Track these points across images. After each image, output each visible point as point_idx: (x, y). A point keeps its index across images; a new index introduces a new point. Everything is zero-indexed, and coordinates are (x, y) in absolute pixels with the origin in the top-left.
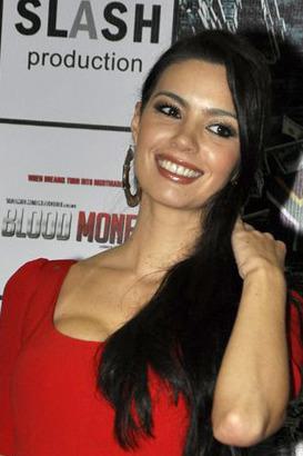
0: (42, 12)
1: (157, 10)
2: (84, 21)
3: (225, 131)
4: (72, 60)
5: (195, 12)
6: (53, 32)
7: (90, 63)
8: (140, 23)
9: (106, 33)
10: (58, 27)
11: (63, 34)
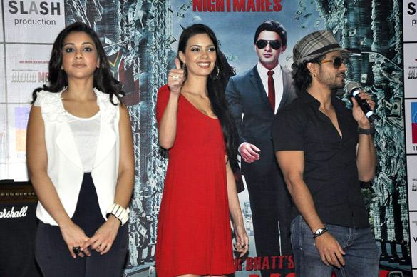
0: (18, 6)
1: (58, 4)
2: (33, 8)
3: (88, 49)
6: (23, 12)
7: (37, 22)
8: (53, 9)
9: (41, 12)
10: (24, 11)
11: (26, 13)
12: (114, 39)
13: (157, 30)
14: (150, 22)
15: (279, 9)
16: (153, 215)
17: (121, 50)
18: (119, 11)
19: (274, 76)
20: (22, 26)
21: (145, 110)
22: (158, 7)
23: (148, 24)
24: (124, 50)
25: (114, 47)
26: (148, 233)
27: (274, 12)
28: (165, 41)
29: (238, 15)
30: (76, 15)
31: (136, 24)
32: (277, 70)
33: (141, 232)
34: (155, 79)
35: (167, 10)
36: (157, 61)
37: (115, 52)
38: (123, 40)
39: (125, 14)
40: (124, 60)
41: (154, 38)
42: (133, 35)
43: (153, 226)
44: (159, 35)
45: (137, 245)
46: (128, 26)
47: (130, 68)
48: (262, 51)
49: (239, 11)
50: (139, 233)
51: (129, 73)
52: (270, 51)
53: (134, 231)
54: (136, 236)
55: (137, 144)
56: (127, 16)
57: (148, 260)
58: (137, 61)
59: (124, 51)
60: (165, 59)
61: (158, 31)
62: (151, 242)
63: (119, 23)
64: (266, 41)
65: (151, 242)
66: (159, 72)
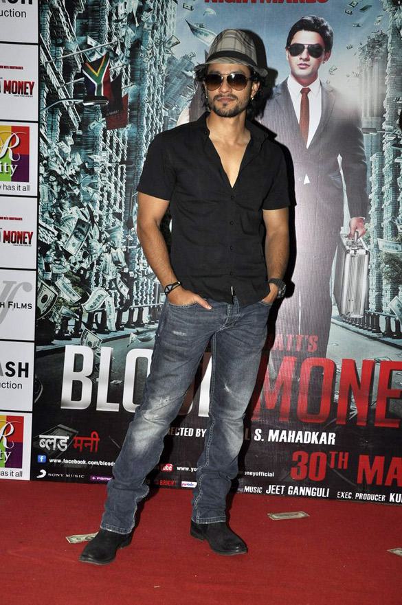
12: (99, 39)
13: (155, 27)
14: (147, 16)
16: (138, 271)
17: (107, 55)
19: (310, 96)
21: (135, 135)
23: (144, 19)
24: (111, 55)
25: (98, 50)
26: (130, 293)
28: (164, 42)
31: (128, 20)
32: (315, 87)
33: (122, 290)
34: (149, 95)
36: (153, 70)
37: (99, 57)
38: (110, 40)
39: (115, 5)
40: (109, 67)
41: (150, 38)
42: (123, 34)
43: (137, 284)
44: (157, 34)
45: (116, 306)
46: (117, 21)
47: (118, 79)
48: (296, 60)
50: (119, 291)
51: (114, 86)
52: (307, 60)
53: (113, 289)
54: (116, 295)
55: (121, 180)
56: (117, 8)
57: (128, 325)
58: (126, 70)
59: (111, 55)
60: (164, 68)
61: (157, 29)
62: (134, 304)
63: (106, 17)
64: (303, 46)
65: (134, 304)
66: (154, 85)
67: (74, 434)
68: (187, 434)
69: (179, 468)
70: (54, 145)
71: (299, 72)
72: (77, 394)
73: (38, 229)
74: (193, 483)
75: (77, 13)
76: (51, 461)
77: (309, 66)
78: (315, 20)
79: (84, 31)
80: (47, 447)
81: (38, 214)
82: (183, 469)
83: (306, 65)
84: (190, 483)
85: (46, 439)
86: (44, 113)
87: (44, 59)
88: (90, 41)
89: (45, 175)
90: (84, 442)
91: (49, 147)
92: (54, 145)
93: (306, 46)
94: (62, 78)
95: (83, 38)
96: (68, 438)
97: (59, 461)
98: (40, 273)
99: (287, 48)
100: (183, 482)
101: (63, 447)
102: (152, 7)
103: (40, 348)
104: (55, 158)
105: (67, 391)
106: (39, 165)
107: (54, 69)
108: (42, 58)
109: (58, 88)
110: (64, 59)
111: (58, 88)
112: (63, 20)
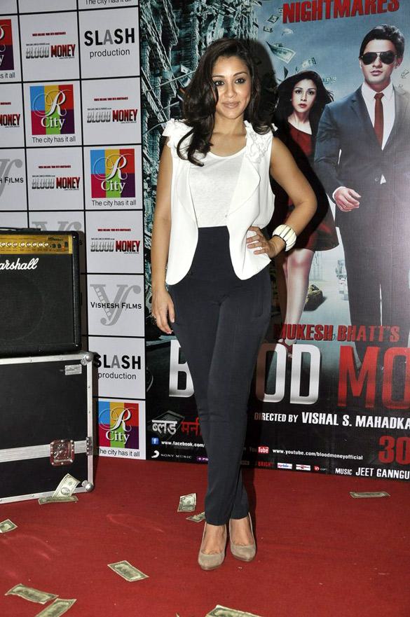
0: (93, 36)
4: (105, 53)
5: (146, 29)
6: (98, 43)
7: (111, 54)
10: (99, 41)
15: (397, 7)
18: (197, 32)
19: (383, 100)
20: (95, 58)
22: (241, 22)
27: (388, 12)
29: (341, 22)
30: (150, 41)
32: (388, 92)
35: (252, 24)
48: (369, 67)
49: (342, 16)
52: (380, 66)
56: (205, 37)
63: (197, 47)
67: (182, 419)
68: (281, 419)
69: (274, 451)
70: (155, 163)
71: (373, 79)
72: (182, 384)
73: (144, 238)
74: (288, 464)
75: (172, 45)
76: (163, 443)
77: (382, 72)
78: (387, 29)
79: (178, 60)
80: (159, 430)
81: (144, 225)
82: (278, 451)
83: (379, 71)
84: (285, 464)
85: (158, 424)
86: (146, 136)
87: (145, 89)
88: (184, 69)
89: (148, 191)
90: (191, 426)
91: (151, 166)
92: (155, 163)
93: (378, 54)
94: (160, 103)
95: (178, 67)
96: (176, 422)
97: (170, 443)
98: (147, 277)
99: (360, 57)
100: (279, 464)
101: (173, 431)
102: (236, 33)
103: (150, 343)
104: (156, 175)
105: (174, 381)
106: (143, 182)
107: (153, 97)
108: (143, 87)
109: (157, 113)
110: (161, 87)
111: (157, 113)
112: (160, 53)
